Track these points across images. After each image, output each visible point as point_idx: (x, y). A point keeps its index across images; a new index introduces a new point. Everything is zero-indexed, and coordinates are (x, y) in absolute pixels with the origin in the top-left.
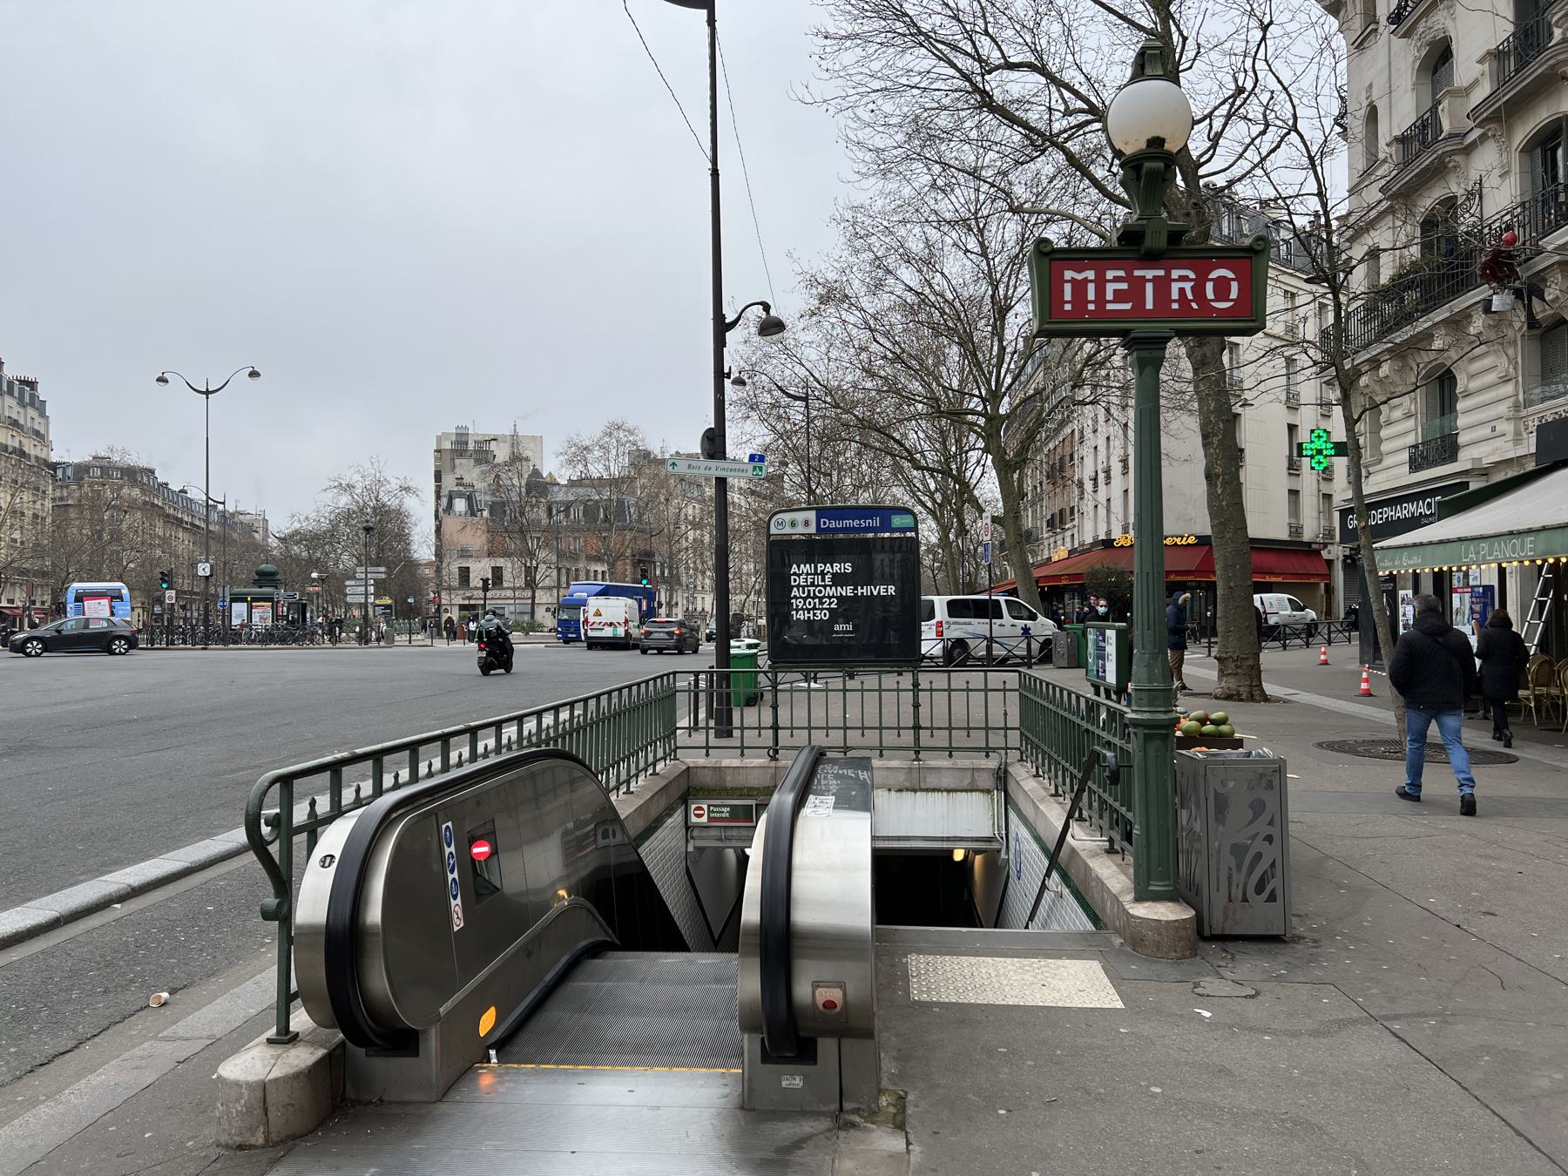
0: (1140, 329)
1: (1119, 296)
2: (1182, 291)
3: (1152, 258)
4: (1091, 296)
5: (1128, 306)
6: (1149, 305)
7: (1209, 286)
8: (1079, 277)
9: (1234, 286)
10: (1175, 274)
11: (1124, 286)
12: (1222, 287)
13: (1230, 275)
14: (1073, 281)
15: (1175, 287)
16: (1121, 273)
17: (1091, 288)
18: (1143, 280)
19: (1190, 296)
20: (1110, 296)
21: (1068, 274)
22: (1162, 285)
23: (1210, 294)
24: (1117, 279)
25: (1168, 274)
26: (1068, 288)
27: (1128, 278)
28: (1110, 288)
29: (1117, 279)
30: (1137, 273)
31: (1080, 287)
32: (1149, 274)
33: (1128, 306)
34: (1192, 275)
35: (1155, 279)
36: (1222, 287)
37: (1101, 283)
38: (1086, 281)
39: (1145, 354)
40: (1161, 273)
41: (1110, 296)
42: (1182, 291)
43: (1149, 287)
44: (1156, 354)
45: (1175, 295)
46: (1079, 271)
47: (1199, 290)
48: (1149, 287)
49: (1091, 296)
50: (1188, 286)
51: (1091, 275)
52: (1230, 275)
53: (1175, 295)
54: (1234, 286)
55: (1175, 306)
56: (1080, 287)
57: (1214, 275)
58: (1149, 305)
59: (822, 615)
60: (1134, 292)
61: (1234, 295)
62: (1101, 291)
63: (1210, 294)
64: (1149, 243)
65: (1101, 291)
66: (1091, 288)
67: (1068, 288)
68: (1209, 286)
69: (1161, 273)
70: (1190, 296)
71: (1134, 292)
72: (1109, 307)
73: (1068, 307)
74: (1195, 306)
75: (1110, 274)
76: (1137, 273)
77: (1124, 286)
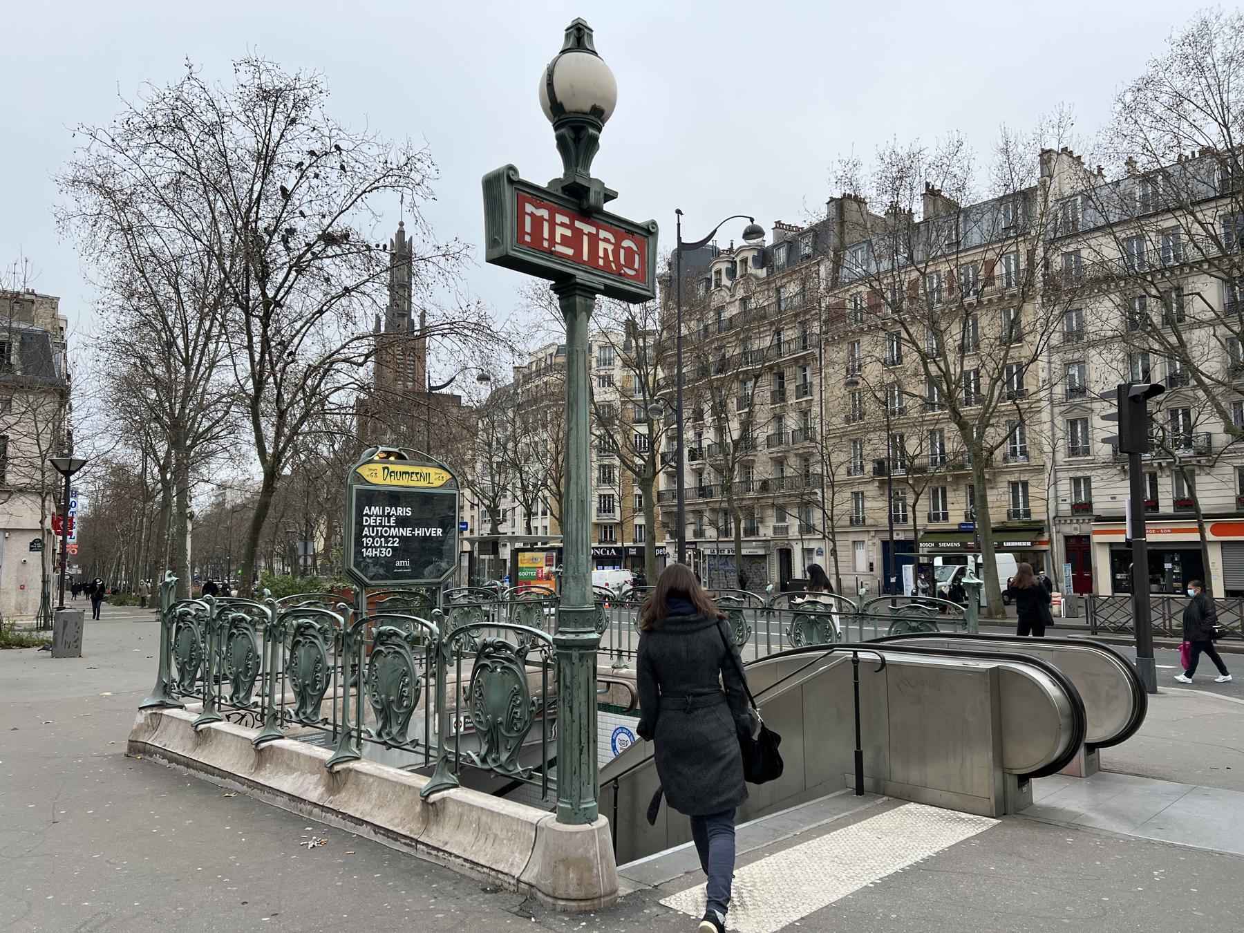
1: (565, 241)
2: (606, 250)
5: (570, 252)
6: (585, 257)
7: (622, 252)
11: (568, 233)
15: (602, 245)
16: (566, 220)
20: (558, 239)
22: (594, 240)
24: (563, 225)
28: (559, 231)
29: (563, 225)
32: (587, 228)
33: (570, 252)
40: (593, 230)
41: (558, 239)
42: (606, 250)
45: (601, 254)
47: (616, 252)
49: (546, 235)
50: (610, 248)
53: (601, 254)
58: (585, 257)
59: (388, 553)
66: (546, 225)
67: (528, 219)
71: (574, 241)
72: (559, 248)
76: (578, 224)
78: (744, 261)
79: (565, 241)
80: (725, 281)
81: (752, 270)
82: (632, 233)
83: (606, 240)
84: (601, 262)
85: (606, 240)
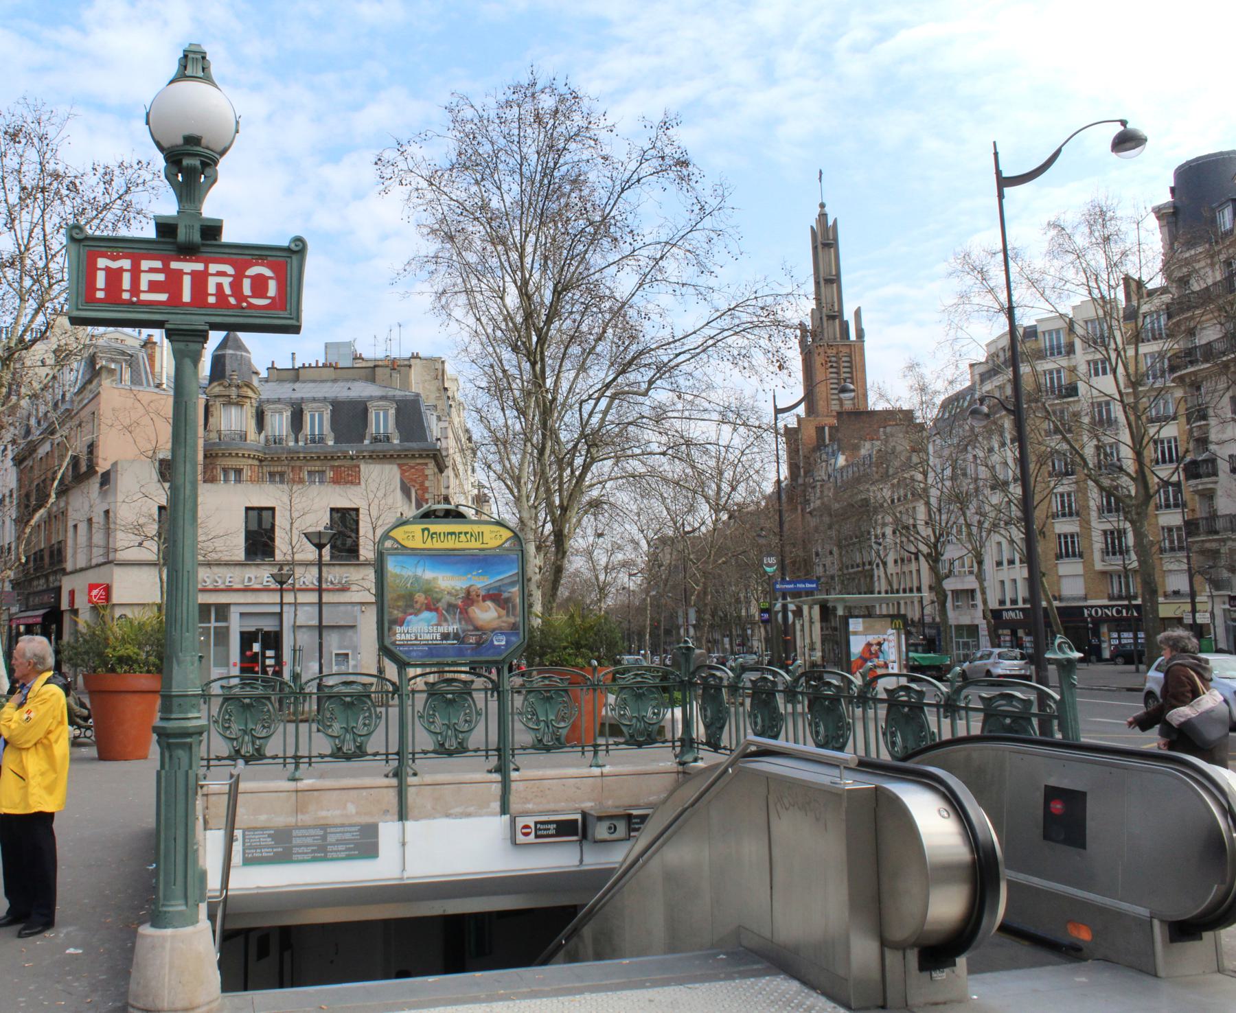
0: (176, 320)
1: (154, 287)
2: (219, 286)
3: (188, 251)
5: (163, 297)
6: (186, 297)
8: (115, 265)
10: (213, 268)
11: (161, 277)
12: (259, 285)
13: (267, 272)
14: (107, 269)
16: (158, 264)
17: (126, 277)
18: (180, 273)
19: (228, 291)
21: (102, 262)
22: (200, 280)
23: (247, 291)
24: (152, 270)
25: (206, 267)
27: (165, 269)
28: (145, 279)
29: (152, 270)
30: (174, 265)
31: (114, 276)
32: (188, 267)
33: (163, 297)
34: (229, 270)
35: (194, 274)
36: (259, 285)
37: (136, 272)
38: (121, 270)
39: (181, 345)
40: (199, 267)
41: (144, 286)
42: (219, 286)
43: (187, 281)
44: (193, 346)
45: (212, 289)
46: (114, 259)
47: (236, 286)
48: (187, 281)
50: (226, 282)
51: (126, 264)
52: (267, 272)
55: (212, 300)
56: (114, 276)
57: (253, 271)
58: (186, 297)
60: (172, 282)
63: (247, 291)
64: (182, 235)
66: (126, 277)
69: (199, 267)
70: (228, 291)
72: (143, 297)
73: (100, 295)
74: (232, 301)
75: (145, 265)
76: (174, 265)
79: (154, 287)
82: (261, 257)
84: (212, 300)
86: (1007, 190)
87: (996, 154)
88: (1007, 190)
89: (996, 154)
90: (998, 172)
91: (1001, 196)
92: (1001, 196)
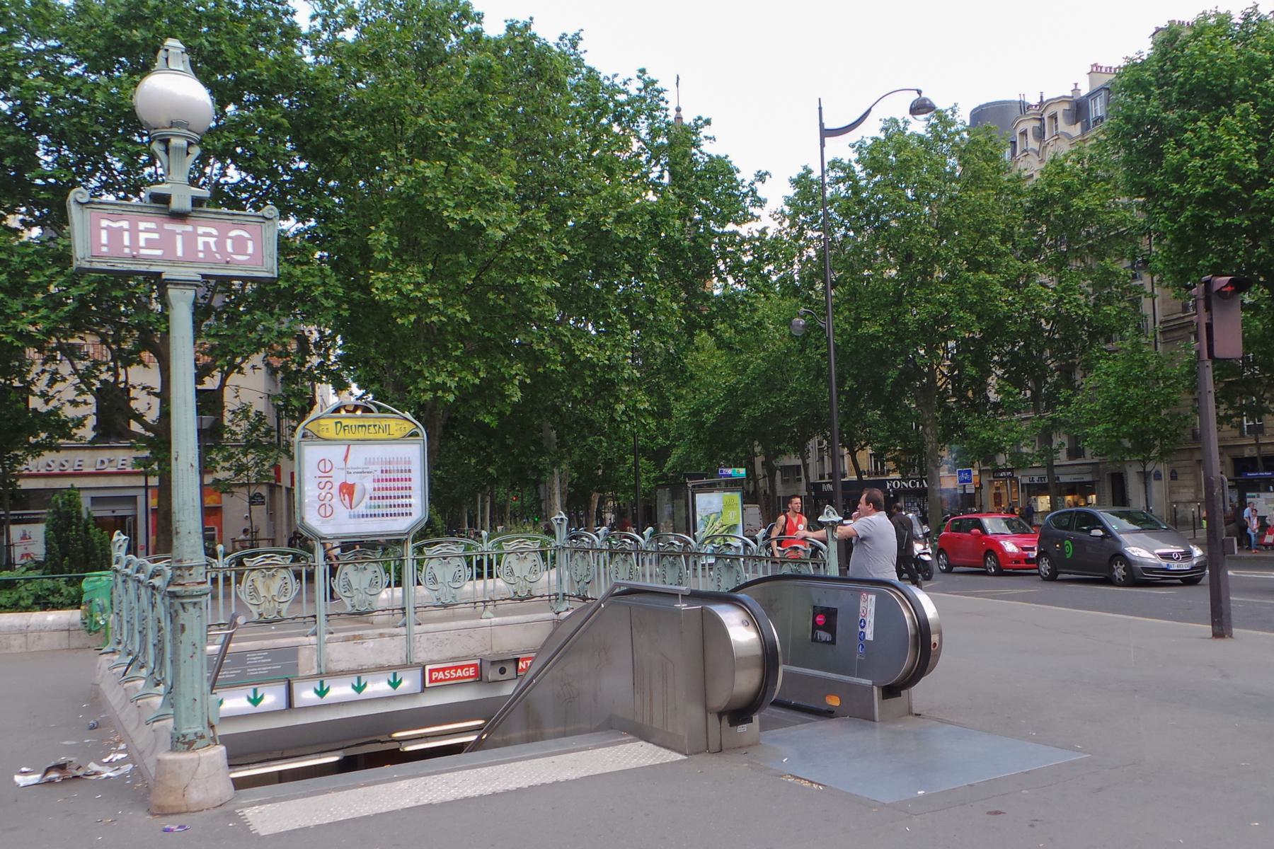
1: (150, 244)
2: (206, 244)
4: (127, 242)
7: (229, 243)
9: (250, 244)
10: (201, 230)
11: (156, 236)
15: (201, 240)
16: (152, 225)
17: (126, 235)
18: (174, 233)
20: (142, 243)
21: (104, 223)
23: (230, 249)
24: (147, 230)
25: (195, 229)
26: (104, 235)
29: (147, 230)
34: (214, 232)
35: (183, 233)
37: (134, 233)
38: (122, 229)
41: (142, 243)
42: (206, 244)
43: (179, 239)
45: (201, 247)
48: (179, 239)
49: (127, 242)
50: (212, 240)
51: (125, 224)
53: (201, 247)
54: (250, 244)
55: (201, 255)
61: (250, 250)
62: (134, 239)
63: (230, 249)
65: (134, 239)
66: (126, 235)
67: (104, 235)
68: (229, 243)
72: (143, 252)
74: (218, 256)
75: (142, 225)
77: (156, 236)
78: (1054, 117)
80: (1033, 144)
81: (1062, 126)
83: (205, 234)
85: (205, 234)
86: (827, 140)
87: (820, 109)
88: (827, 140)
89: (820, 109)
90: (822, 125)
91: (822, 145)
92: (822, 145)
